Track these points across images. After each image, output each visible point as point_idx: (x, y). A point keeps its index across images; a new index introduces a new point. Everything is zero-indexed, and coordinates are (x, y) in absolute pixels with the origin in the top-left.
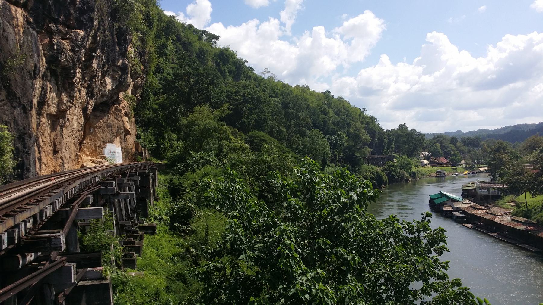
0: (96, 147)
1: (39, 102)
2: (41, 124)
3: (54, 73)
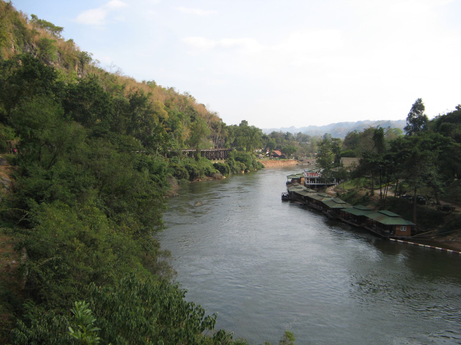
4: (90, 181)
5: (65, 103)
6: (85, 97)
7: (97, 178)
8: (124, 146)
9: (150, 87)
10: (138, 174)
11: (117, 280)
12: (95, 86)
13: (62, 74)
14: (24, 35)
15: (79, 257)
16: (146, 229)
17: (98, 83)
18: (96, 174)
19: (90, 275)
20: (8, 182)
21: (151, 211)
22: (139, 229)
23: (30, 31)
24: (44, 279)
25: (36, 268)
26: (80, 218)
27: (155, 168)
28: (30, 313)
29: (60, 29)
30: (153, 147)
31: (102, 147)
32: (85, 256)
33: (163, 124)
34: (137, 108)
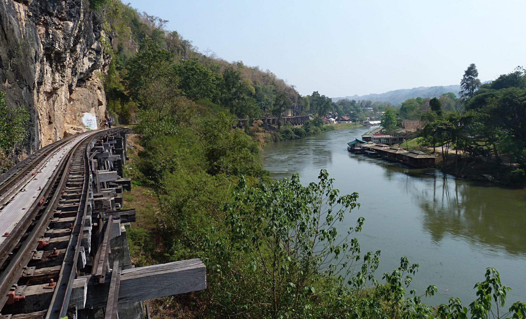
0: (75, 116)
1: (38, 83)
3: (49, 58)
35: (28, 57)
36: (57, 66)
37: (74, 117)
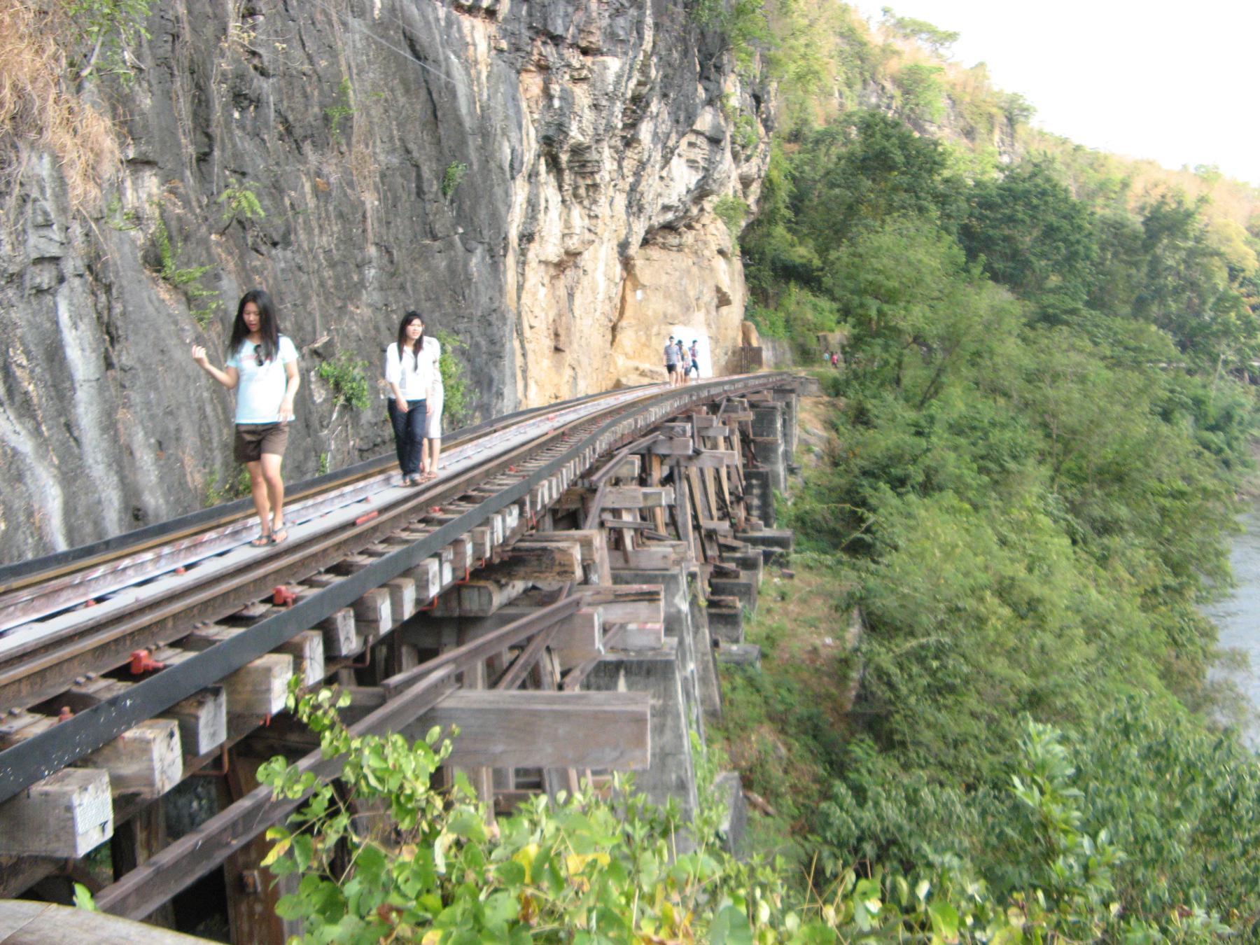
0: (648, 337)
2: (528, 285)
3: (554, 164)
4: (1031, 443)
5: (966, 234)
6: (1020, 216)
7: (1048, 436)
8: (1126, 348)
9: (1204, 180)
10: (1165, 429)
11: (1090, 715)
12: (1047, 186)
13: (957, 154)
14: (862, 60)
15: (994, 644)
16: (1180, 584)
17: (1055, 177)
18: (1045, 425)
19: (1019, 694)
20: (820, 438)
21: (1196, 535)
22: (1158, 582)
23: (877, 50)
24: (904, 690)
25: (885, 660)
26: (1003, 542)
27: (1213, 411)
28: (864, 771)
29: (952, 37)
30: (1209, 354)
31: (1066, 351)
32: (1011, 641)
33: (1241, 285)
34: (1165, 241)
35: (492, 165)
36: (576, 188)
37: (643, 339)
